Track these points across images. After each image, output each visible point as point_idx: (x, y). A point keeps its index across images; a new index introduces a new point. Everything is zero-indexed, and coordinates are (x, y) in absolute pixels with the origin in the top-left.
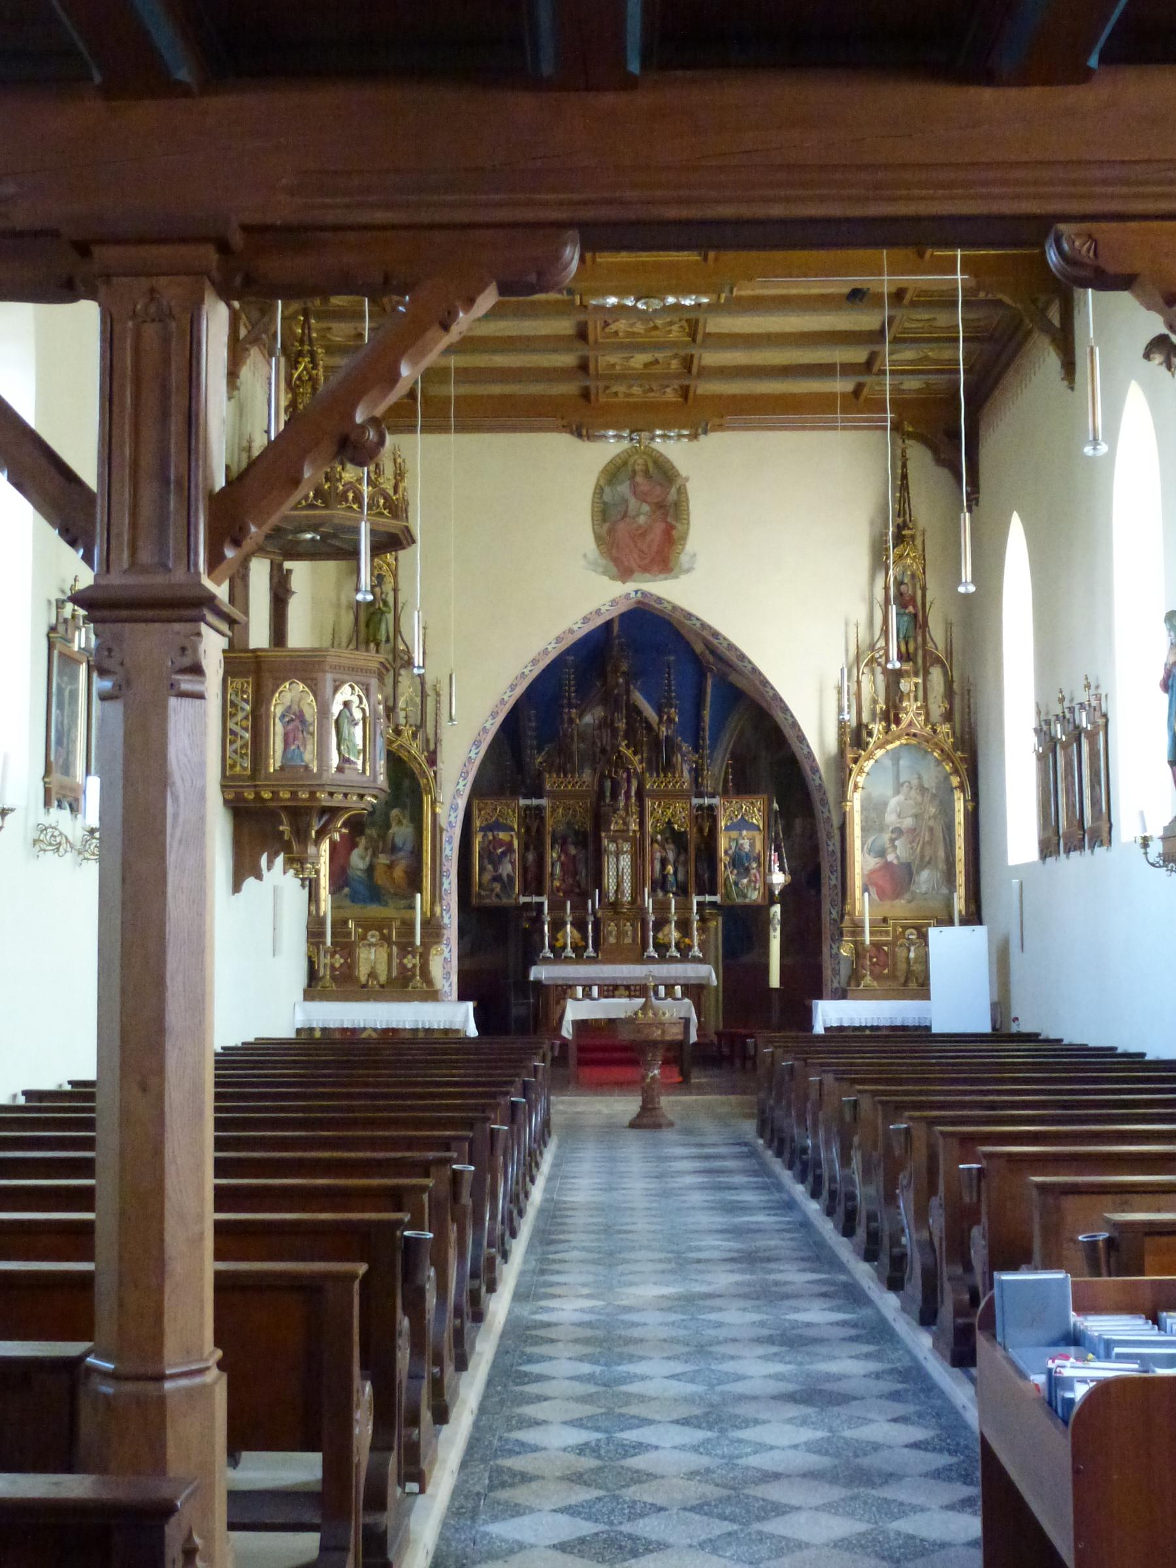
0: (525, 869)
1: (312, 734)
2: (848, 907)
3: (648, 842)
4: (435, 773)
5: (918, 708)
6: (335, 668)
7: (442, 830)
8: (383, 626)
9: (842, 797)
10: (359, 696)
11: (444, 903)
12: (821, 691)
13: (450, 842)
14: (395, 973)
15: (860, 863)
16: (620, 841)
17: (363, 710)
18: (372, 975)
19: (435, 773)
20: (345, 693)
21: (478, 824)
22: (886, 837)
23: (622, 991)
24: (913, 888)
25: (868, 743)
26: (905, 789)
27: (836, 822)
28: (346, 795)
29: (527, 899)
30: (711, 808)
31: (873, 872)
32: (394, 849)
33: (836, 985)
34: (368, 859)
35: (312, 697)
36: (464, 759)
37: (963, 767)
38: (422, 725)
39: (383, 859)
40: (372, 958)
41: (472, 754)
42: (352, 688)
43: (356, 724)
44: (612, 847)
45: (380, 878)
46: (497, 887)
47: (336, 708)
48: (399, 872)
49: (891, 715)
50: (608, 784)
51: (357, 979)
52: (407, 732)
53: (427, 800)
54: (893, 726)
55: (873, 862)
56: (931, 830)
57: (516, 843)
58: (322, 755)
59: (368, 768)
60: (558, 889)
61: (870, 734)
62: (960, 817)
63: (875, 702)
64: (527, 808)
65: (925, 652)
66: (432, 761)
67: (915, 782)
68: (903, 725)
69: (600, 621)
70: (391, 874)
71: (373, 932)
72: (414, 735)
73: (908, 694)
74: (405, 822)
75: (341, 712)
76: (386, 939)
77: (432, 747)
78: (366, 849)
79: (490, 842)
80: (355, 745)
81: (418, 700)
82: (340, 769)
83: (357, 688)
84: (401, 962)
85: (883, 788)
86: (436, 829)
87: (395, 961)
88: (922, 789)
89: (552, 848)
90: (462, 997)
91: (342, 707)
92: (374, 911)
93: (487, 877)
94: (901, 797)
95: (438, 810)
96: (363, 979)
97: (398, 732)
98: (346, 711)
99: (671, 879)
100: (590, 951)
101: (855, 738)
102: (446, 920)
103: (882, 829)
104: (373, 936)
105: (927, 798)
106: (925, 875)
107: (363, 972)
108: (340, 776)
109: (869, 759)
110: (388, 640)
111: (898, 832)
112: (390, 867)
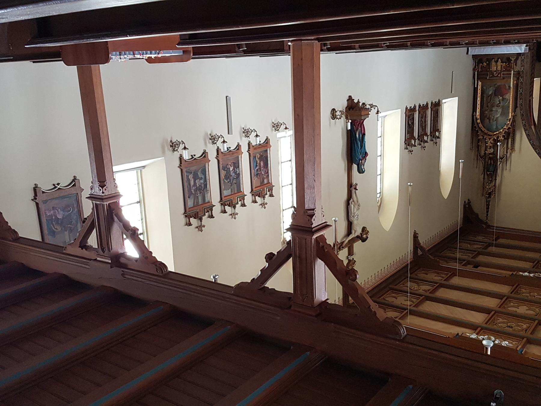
2: (515, 82)
9: (514, 117)
12: (520, 150)
15: (510, 96)
22: (501, 105)
24: (494, 89)
27: (518, 109)
31: (507, 94)
33: (523, 57)
37: (476, 125)
49: (496, 141)
55: (507, 97)
56: (487, 106)
61: (503, 136)
62: (478, 110)
65: (485, 160)
67: (491, 121)
85: (501, 120)
88: (489, 119)
94: (496, 117)
101: (510, 135)
103: (503, 107)
105: (488, 116)
106: (490, 93)
111: (498, 106)
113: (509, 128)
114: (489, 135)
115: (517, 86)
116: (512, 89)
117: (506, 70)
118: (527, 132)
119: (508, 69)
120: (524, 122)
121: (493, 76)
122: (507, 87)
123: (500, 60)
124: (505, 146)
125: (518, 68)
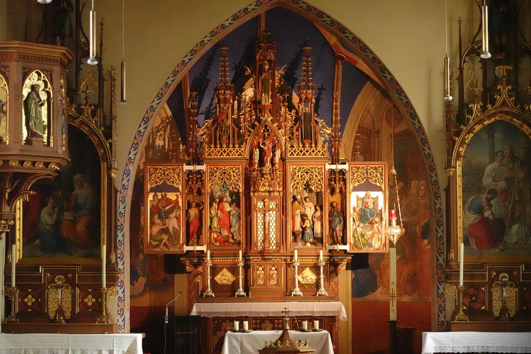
0: (188, 225)
1: (5, 113)
2: (452, 255)
3: (290, 200)
4: (111, 144)
5: (509, 90)
6: (23, 57)
7: (116, 191)
8: (68, 23)
9: (449, 165)
10: (45, 81)
11: (119, 252)
12: (429, 77)
13: (123, 203)
14: (77, 310)
16: (266, 200)
17: (48, 93)
18: (60, 311)
19: (111, 144)
20: (33, 79)
21: (149, 187)
22: (484, 197)
23: (267, 323)
25: (468, 120)
26: (499, 157)
27: (443, 184)
28: (34, 163)
29: (190, 248)
30: (342, 172)
31: (472, 226)
32: (77, 208)
33: (442, 319)
34: (55, 215)
35: (5, 82)
36: (135, 132)
38: (99, 105)
39: (68, 216)
40: (58, 298)
41: (142, 129)
42: (39, 75)
43: (42, 105)
44: (260, 205)
45: (65, 232)
46: (165, 237)
47: (26, 92)
48: (81, 227)
49: (488, 96)
50: (257, 152)
51: (47, 314)
52: (88, 110)
53: (104, 166)
54: (489, 106)
55: (472, 218)
57: (180, 200)
58: (15, 131)
59: (52, 141)
60: (216, 240)
61: (470, 112)
63: (473, 85)
64: (190, 172)
66: (108, 135)
67: (507, 152)
68: (498, 104)
69: (247, 18)
70: (75, 229)
71: (60, 276)
72: (94, 114)
73: (501, 79)
74: (85, 185)
75: (29, 94)
76: (71, 282)
77: (108, 123)
78: (53, 208)
79: (159, 200)
80: (42, 122)
81: (97, 83)
82: (28, 142)
83: (42, 75)
84: (82, 301)
85: (481, 156)
86: (112, 191)
87: (78, 301)
88: (513, 158)
89: (211, 205)
90: (133, 330)
91: (30, 91)
92: (62, 258)
93: (156, 229)
94: (495, 164)
95: (113, 175)
96: (52, 316)
97: (80, 111)
98: (34, 93)
99: (308, 231)
100: (241, 291)
101: (456, 117)
102: (120, 266)
103: (480, 190)
104: (59, 279)
106: (515, 227)
107: (52, 308)
108: (28, 147)
109: (469, 132)
110: (71, 35)
111: (493, 193)
112: (74, 222)
113: (458, 134)
114: (507, 113)
115: (450, 244)
116: (460, 234)
117: (477, 287)
118: (417, 125)
119: (472, 291)
120: (427, 151)
121: (509, 272)
122: (472, 242)
123: (496, 314)
124: (466, 86)
125: (450, 292)
